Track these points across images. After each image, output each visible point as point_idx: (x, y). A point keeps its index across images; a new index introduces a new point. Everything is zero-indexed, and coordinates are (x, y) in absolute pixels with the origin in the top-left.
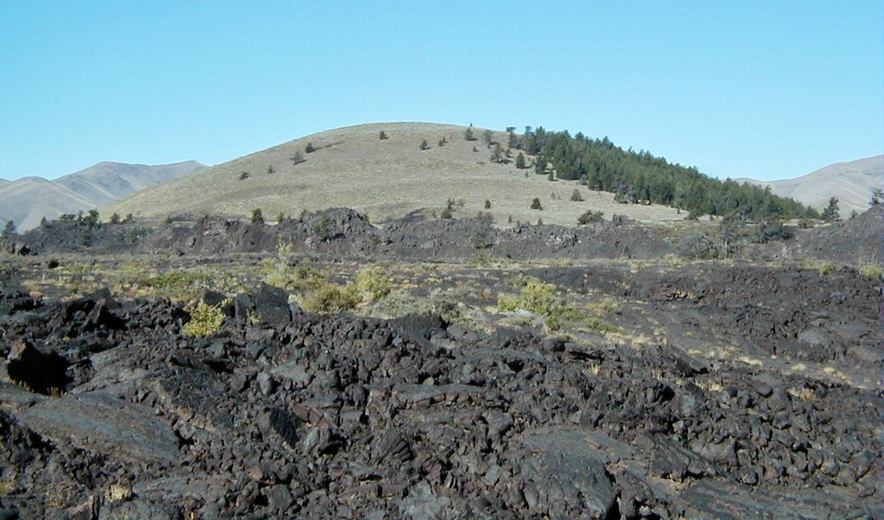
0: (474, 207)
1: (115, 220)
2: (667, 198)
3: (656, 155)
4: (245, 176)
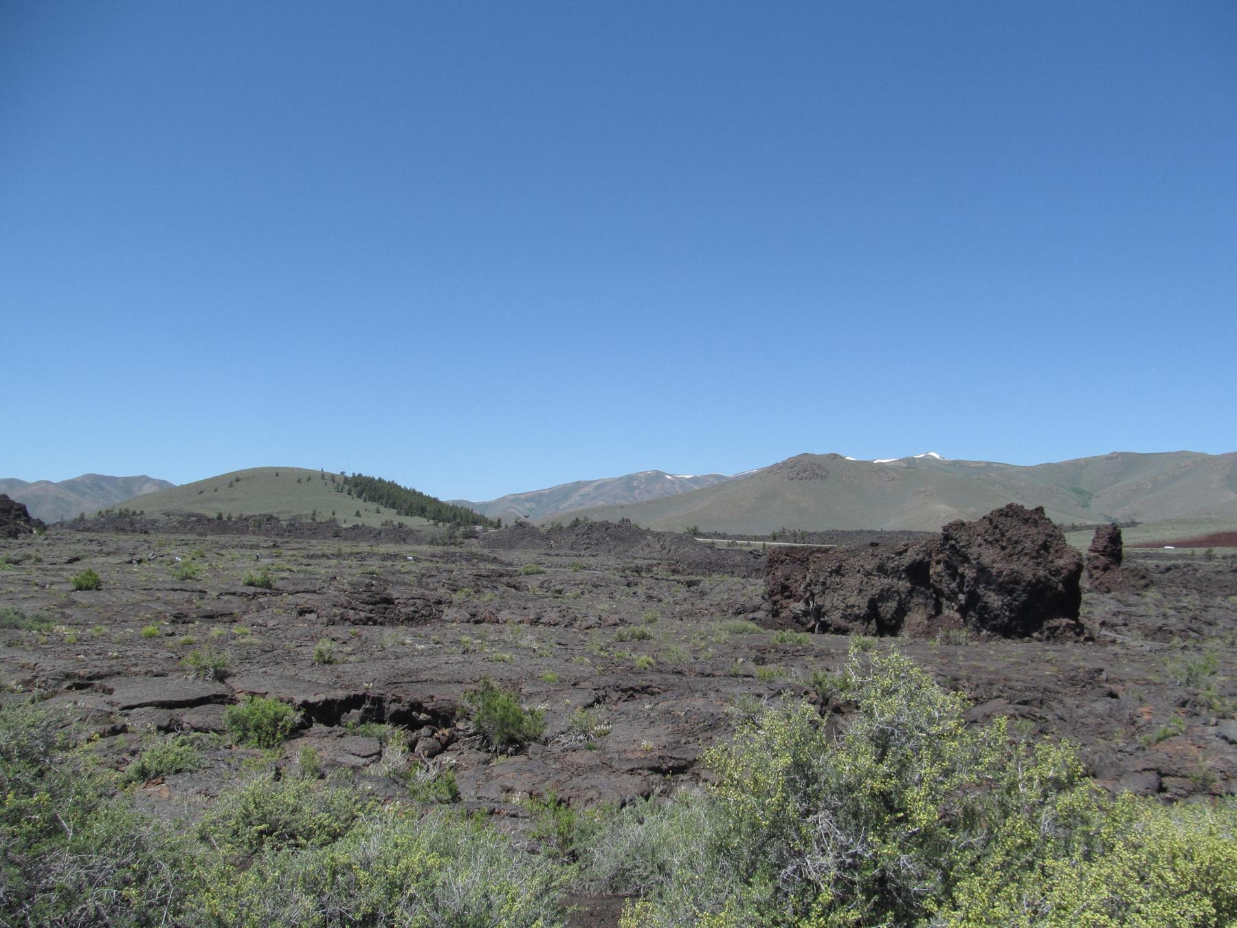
0: (324, 516)
2: (422, 512)
3: (418, 490)
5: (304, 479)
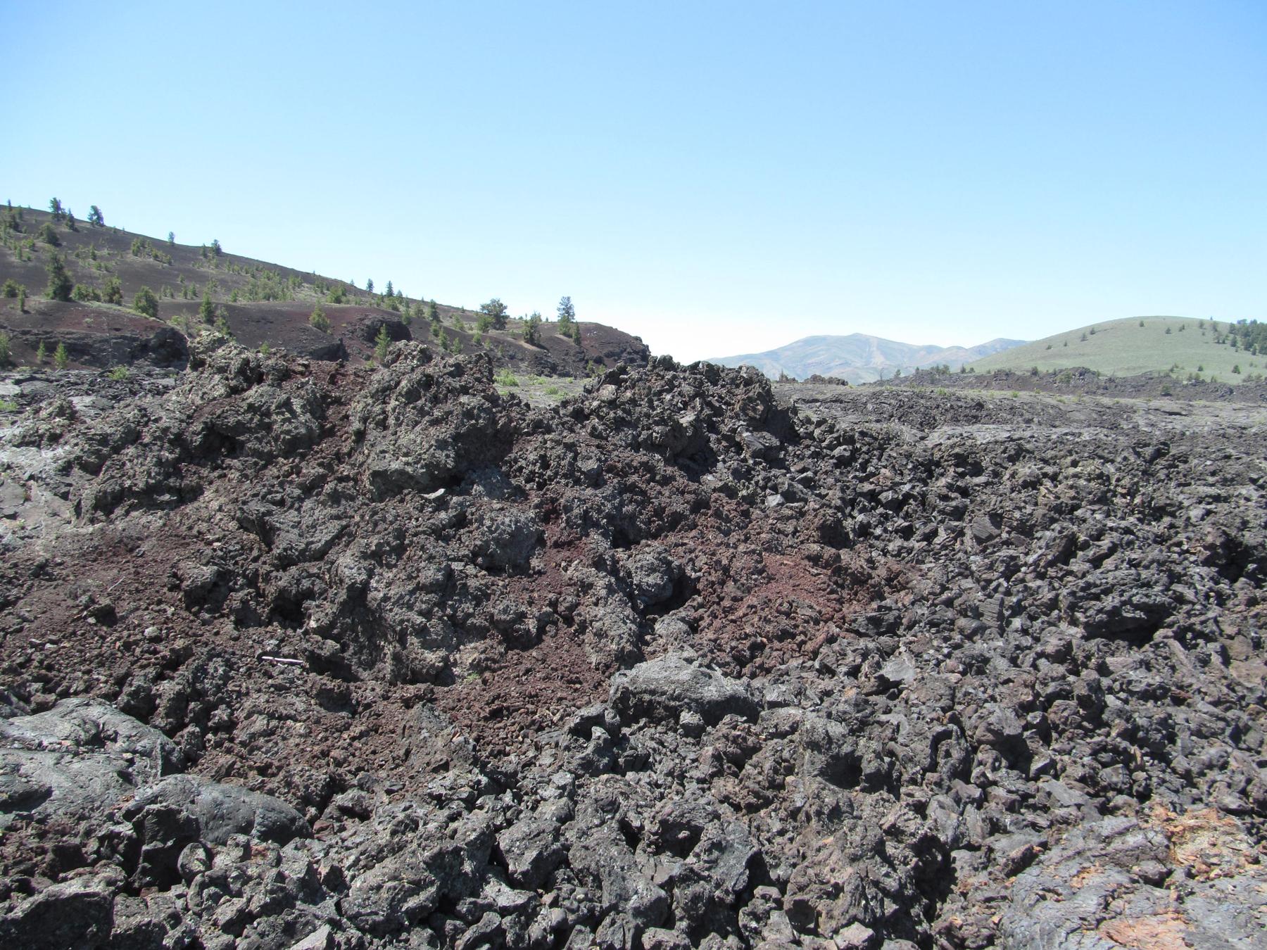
1: (963, 371)
4: (1049, 348)
5: (1175, 329)
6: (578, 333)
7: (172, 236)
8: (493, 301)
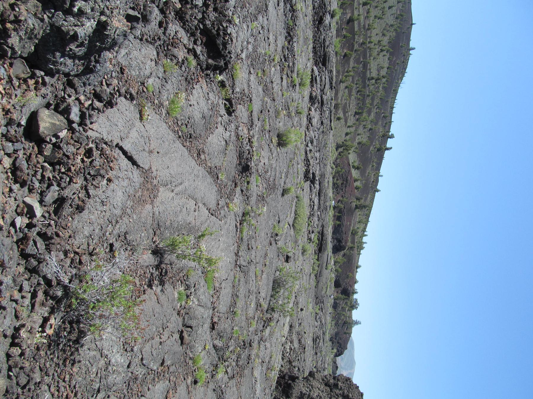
6: (348, 333)
7: (382, 176)
8: (358, 304)
